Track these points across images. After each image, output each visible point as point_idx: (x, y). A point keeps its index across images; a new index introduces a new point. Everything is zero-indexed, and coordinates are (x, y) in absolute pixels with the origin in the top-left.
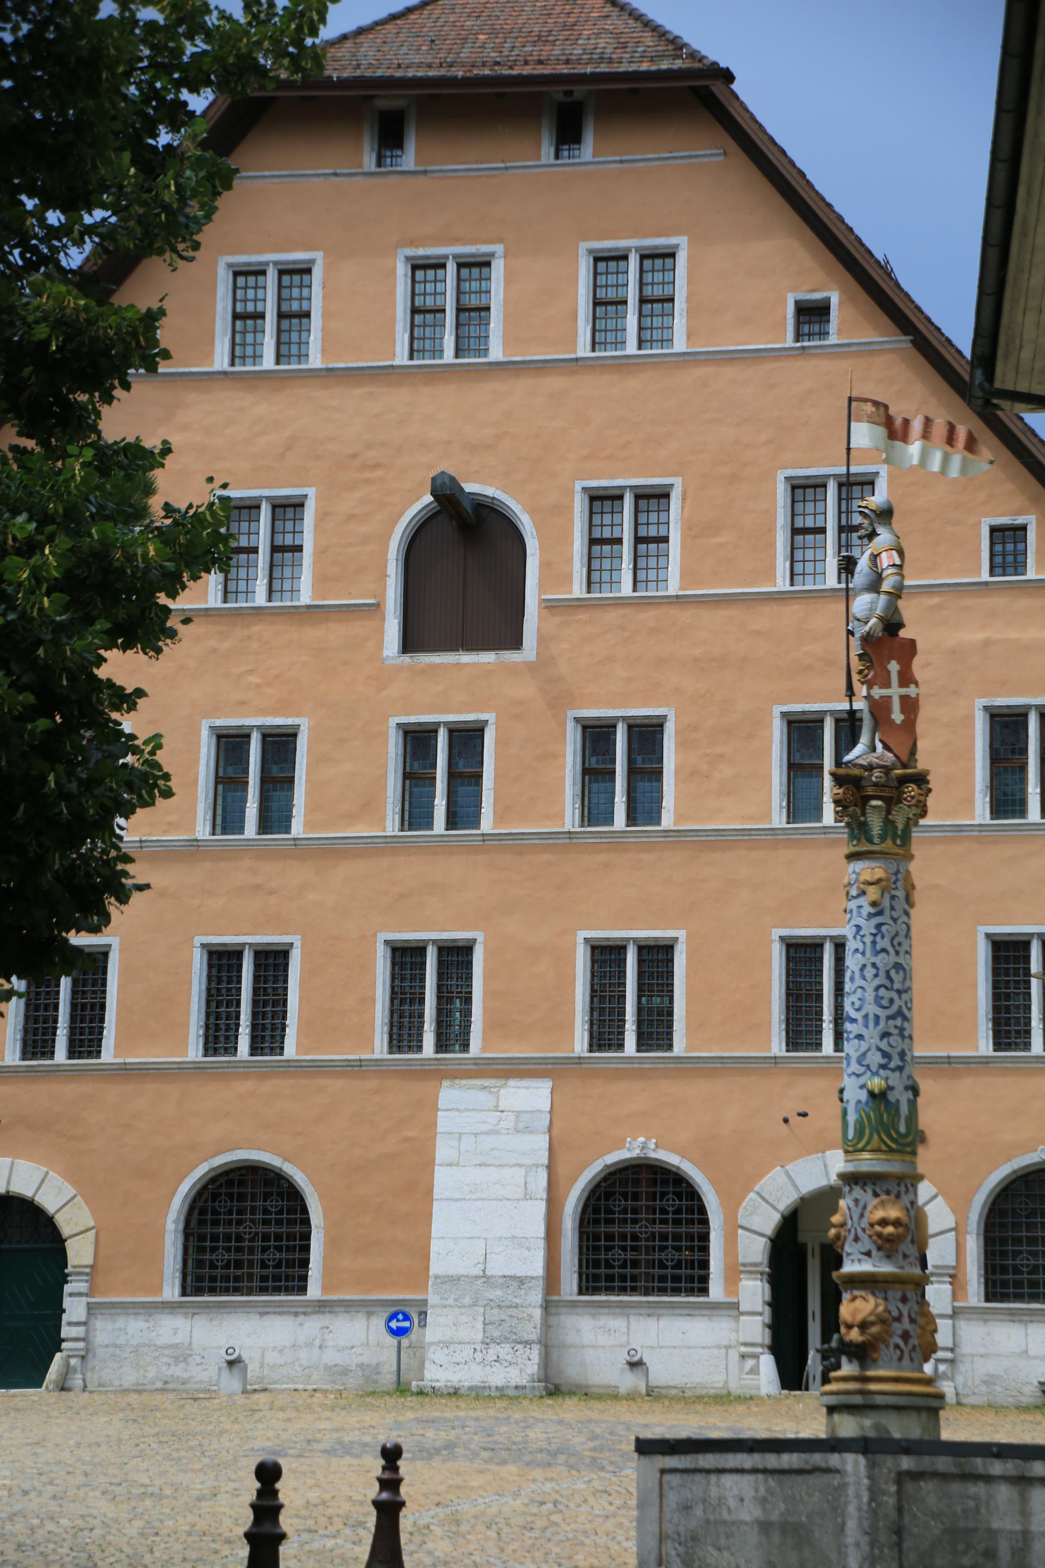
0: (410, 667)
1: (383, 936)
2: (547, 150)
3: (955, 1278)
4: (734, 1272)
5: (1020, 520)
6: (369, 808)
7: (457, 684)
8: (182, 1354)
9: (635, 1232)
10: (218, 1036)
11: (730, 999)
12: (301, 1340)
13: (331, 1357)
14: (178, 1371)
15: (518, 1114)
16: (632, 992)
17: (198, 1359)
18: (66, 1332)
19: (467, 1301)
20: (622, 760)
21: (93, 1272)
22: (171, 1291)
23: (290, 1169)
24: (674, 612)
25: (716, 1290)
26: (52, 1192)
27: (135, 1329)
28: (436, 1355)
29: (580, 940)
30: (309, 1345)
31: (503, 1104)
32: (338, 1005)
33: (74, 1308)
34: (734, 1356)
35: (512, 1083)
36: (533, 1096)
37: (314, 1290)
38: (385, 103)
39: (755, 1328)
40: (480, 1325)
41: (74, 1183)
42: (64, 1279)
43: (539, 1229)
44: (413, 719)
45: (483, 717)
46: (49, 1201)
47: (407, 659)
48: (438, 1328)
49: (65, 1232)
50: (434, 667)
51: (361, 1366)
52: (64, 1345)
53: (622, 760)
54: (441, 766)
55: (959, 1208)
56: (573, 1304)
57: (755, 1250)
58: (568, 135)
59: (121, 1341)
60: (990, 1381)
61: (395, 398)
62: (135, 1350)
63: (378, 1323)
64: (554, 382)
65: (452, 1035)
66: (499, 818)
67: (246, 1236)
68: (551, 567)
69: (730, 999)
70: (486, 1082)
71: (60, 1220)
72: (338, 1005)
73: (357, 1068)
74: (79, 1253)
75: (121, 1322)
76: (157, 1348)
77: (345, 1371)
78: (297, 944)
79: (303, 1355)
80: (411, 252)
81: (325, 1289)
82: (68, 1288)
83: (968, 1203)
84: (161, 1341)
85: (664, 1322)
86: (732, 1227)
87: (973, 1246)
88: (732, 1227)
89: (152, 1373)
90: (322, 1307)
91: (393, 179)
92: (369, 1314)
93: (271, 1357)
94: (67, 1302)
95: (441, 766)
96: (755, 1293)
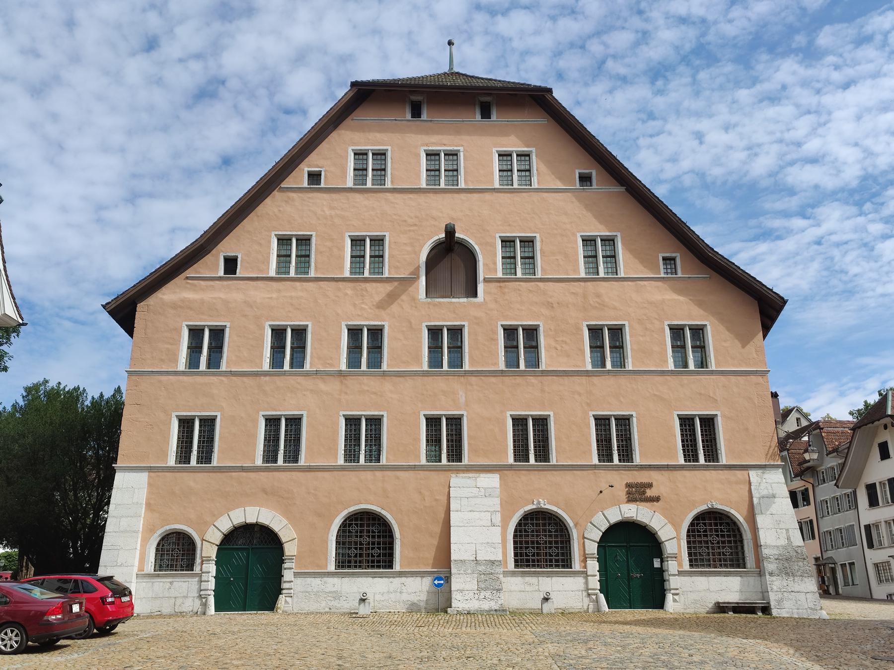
0: (429, 303)
1: (422, 413)
2: (478, 117)
5: (674, 255)
7: (450, 310)
8: (337, 596)
9: (540, 541)
10: (351, 455)
11: (575, 440)
12: (391, 590)
13: (405, 597)
14: (335, 603)
15: (485, 489)
16: (532, 439)
17: (345, 598)
18: (284, 586)
19: (469, 571)
20: (522, 341)
22: (332, 567)
23: (384, 513)
24: (540, 284)
25: (577, 566)
31: (479, 485)
32: (405, 440)
33: (287, 575)
35: (482, 475)
36: (492, 481)
37: (397, 567)
38: (415, 98)
39: (595, 583)
41: (287, 518)
42: (282, 562)
43: (499, 539)
44: (433, 324)
45: (463, 323)
46: (276, 527)
47: (429, 300)
49: (283, 540)
50: (439, 303)
52: (284, 591)
53: (522, 341)
54: (446, 343)
57: (592, 548)
58: (486, 114)
59: (309, 589)
60: (695, 602)
61: (421, 199)
64: (487, 196)
65: (456, 454)
66: (471, 364)
67: (367, 542)
68: (490, 262)
69: (575, 440)
70: (471, 475)
72: (405, 440)
73: (414, 468)
74: (290, 549)
78: (385, 415)
79: (392, 596)
80: (426, 148)
82: (285, 565)
83: (680, 526)
84: (327, 590)
85: (554, 578)
89: (323, 604)
90: (401, 574)
91: (418, 123)
93: (378, 597)
95: (446, 343)
96: (593, 566)
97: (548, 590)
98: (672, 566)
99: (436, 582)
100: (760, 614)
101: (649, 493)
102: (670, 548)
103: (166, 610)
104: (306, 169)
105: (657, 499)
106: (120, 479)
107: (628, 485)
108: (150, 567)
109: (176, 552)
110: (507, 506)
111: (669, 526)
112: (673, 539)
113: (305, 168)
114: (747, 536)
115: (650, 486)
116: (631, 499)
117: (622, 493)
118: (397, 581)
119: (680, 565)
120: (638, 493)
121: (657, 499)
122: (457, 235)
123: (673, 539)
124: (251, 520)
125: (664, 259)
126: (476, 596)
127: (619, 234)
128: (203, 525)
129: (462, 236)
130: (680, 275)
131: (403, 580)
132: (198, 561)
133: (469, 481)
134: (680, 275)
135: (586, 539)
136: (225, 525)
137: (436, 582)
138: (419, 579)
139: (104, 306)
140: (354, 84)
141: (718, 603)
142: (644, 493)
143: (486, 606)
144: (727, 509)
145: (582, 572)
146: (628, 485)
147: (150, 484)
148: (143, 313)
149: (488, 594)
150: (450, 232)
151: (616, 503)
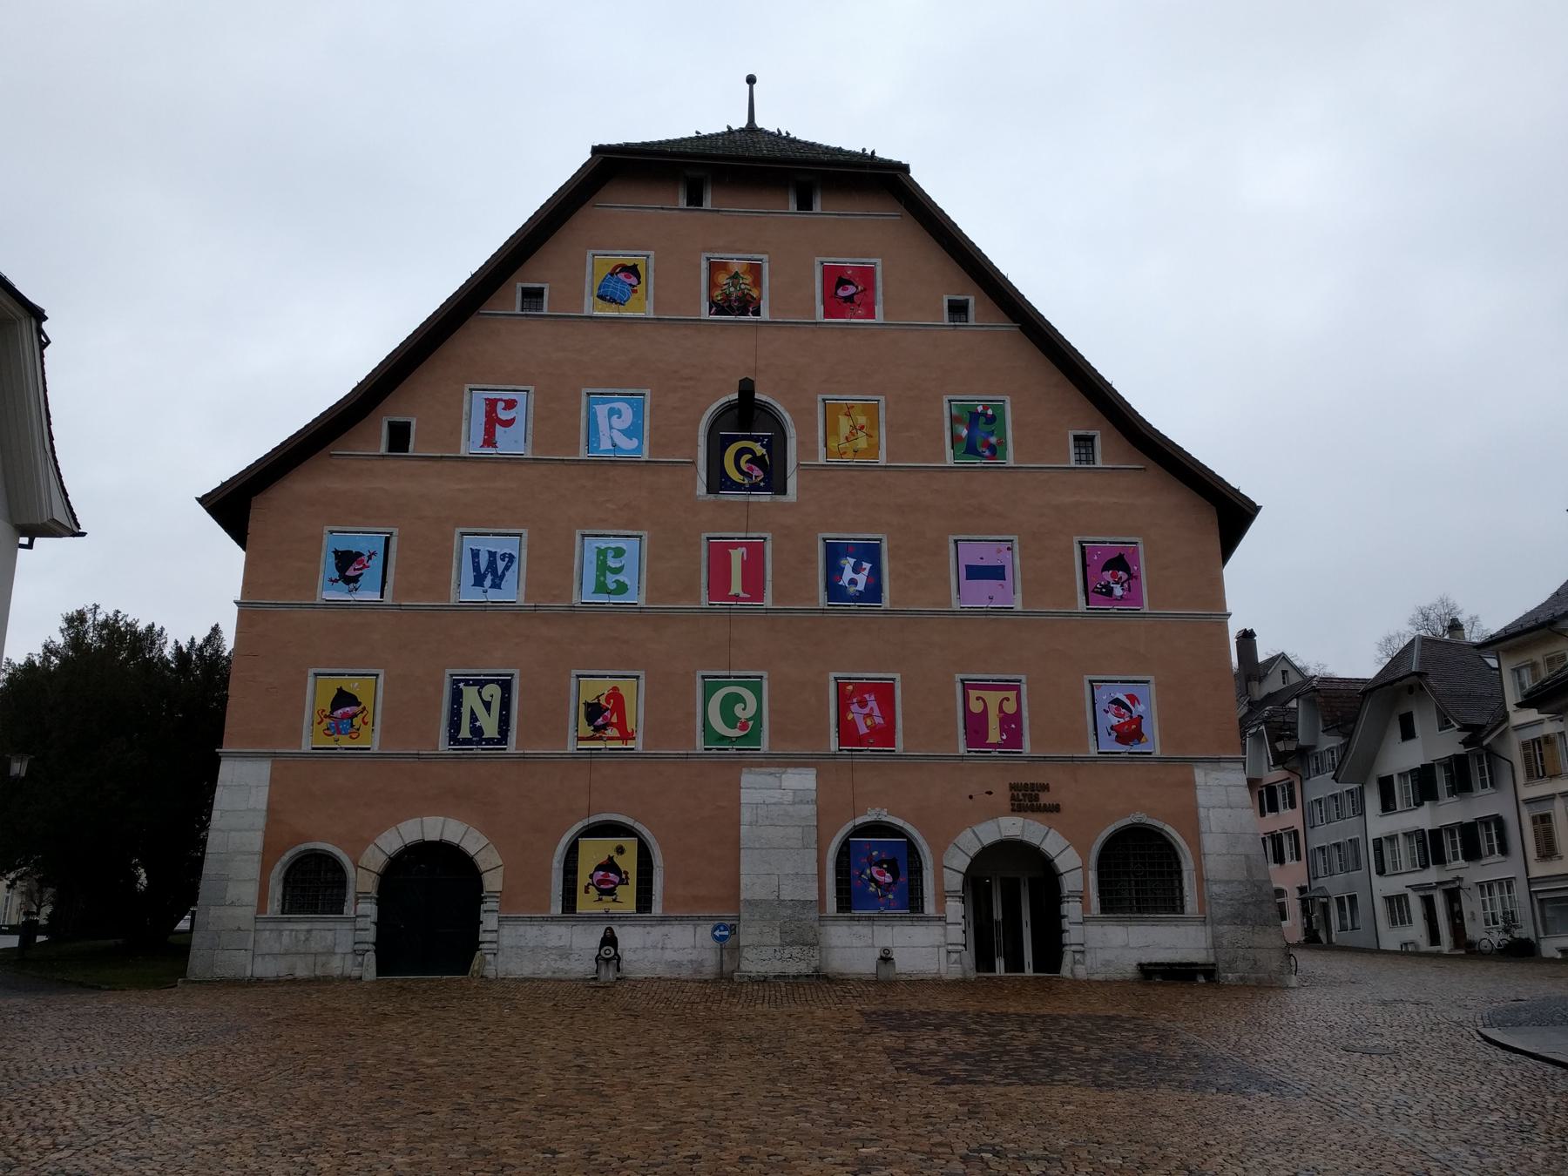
3: (1082, 897)
4: (942, 896)
5: (1091, 433)
6: (691, 590)
8: (565, 953)
13: (669, 955)
14: (561, 964)
15: (795, 791)
18: (483, 937)
21: (504, 897)
25: (930, 908)
26: (473, 842)
27: (531, 934)
28: (748, 954)
29: (831, 678)
30: (655, 947)
33: (489, 921)
34: (943, 952)
35: (789, 770)
36: (803, 780)
39: (956, 934)
40: (777, 934)
41: (488, 835)
42: (481, 901)
43: (812, 868)
47: (712, 496)
48: (747, 936)
49: (482, 868)
51: (691, 961)
55: (1083, 852)
56: (835, 919)
57: (955, 881)
60: (1107, 963)
62: (532, 950)
63: (705, 930)
66: (775, 600)
70: (772, 770)
71: (479, 859)
74: (492, 882)
75: (522, 929)
76: (547, 949)
77: (680, 965)
79: (650, 953)
81: (664, 909)
84: (550, 944)
86: (940, 867)
87: (1093, 876)
88: (940, 867)
89: (544, 965)
90: (663, 920)
92: (695, 926)
94: (483, 916)
97: (888, 944)
98: (1071, 909)
99: (717, 933)
100: (1201, 980)
101: (1045, 799)
102: (1070, 883)
103: (301, 972)
104: (519, 285)
105: (1056, 808)
106: (228, 771)
107: (1013, 787)
108: (274, 906)
109: (312, 884)
110: (825, 815)
111: (1071, 851)
112: (1075, 868)
113: (518, 285)
114: (1188, 866)
115: (1045, 788)
116: (1018, 808)
117: (1003, 796)
118: (657, 932)
119: (1086, 909)
120: (1027, 800)
121: (1056, 808)
122: (757, 396)
123: (1075, 868)
124: (432, 836)
125: (1077, 438)
126: (778, 955)
127: (1008, 399)
128: (359, 844)
129: (763, 398)
130: (1099, 464)
131: (665, 929)
132: (350, 896)
133: (770, 779)
134: (1099, 464)
135: (946, 868)
136: (392, 841)
137: (717, 933)
138: (690, 928)
139: (200, 500)
140: (596, 150)
141: (1140, 965)
142: (1037, 798)
143: (792, 969)
144: (1159, 824)
145: (940, 919)
146: (1013, 787)
147: (273, 780)
148: (261, 514)
149: (796, 951)
150: (747, 389)
151: (994, 814)
